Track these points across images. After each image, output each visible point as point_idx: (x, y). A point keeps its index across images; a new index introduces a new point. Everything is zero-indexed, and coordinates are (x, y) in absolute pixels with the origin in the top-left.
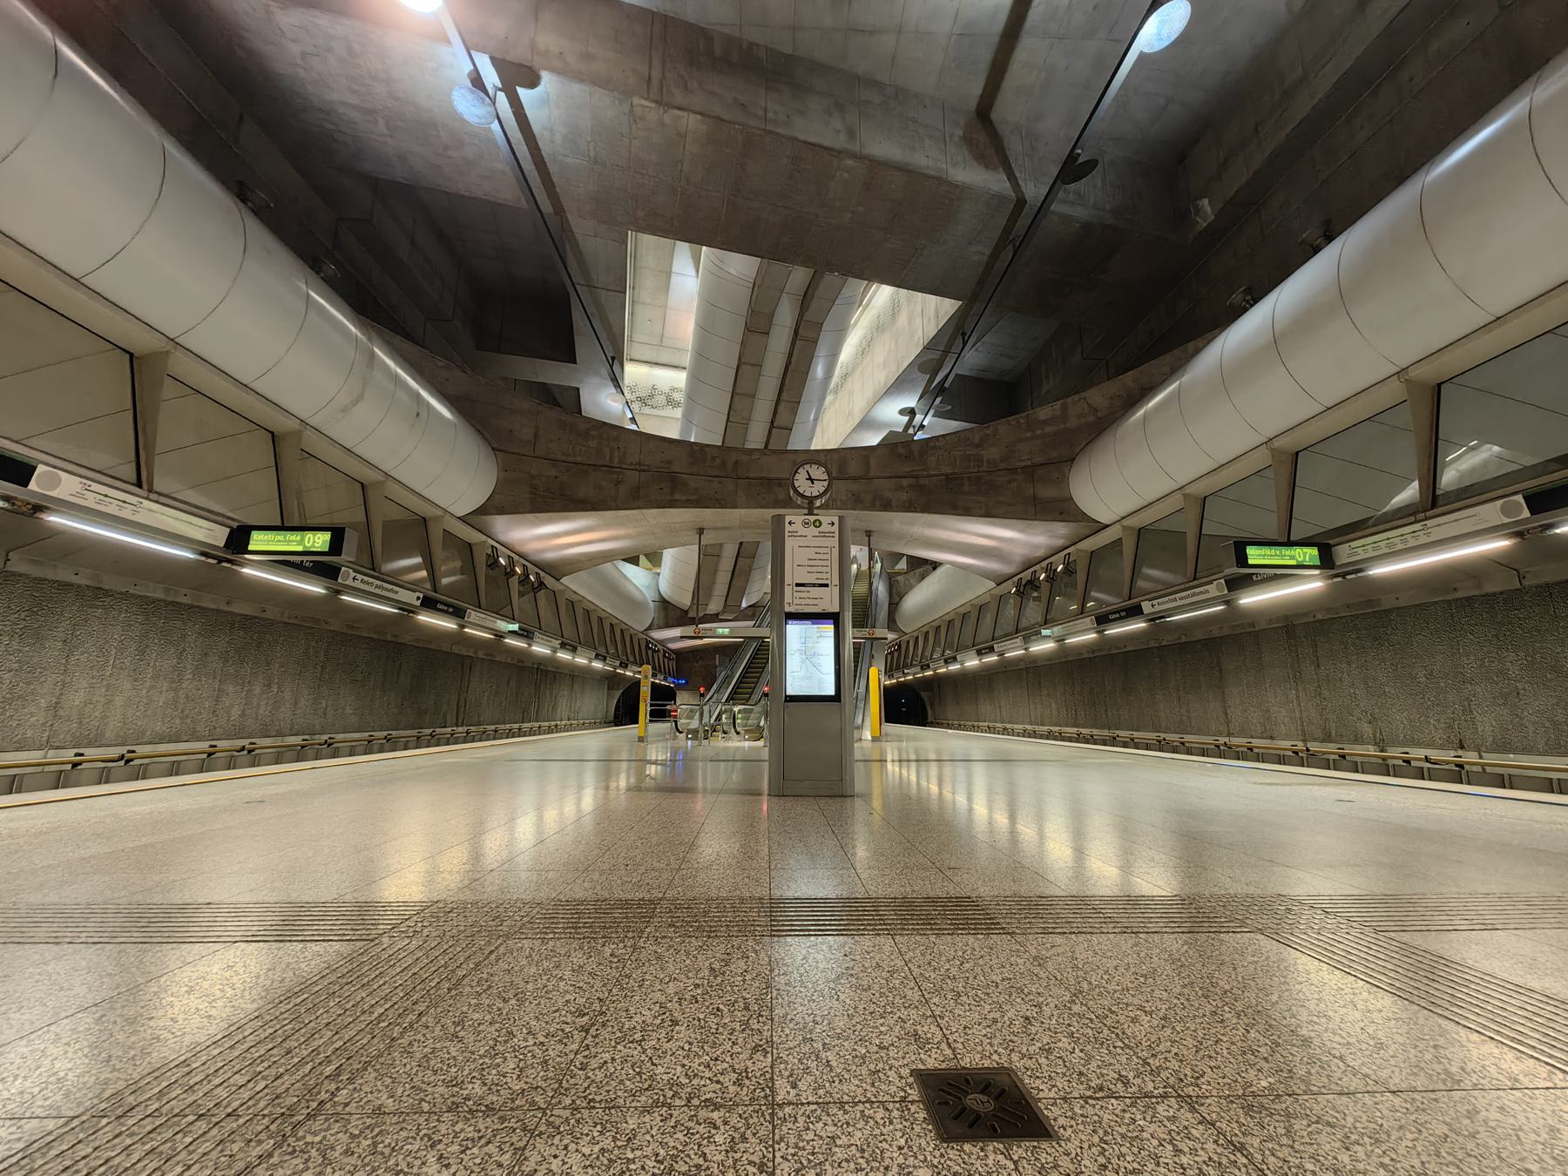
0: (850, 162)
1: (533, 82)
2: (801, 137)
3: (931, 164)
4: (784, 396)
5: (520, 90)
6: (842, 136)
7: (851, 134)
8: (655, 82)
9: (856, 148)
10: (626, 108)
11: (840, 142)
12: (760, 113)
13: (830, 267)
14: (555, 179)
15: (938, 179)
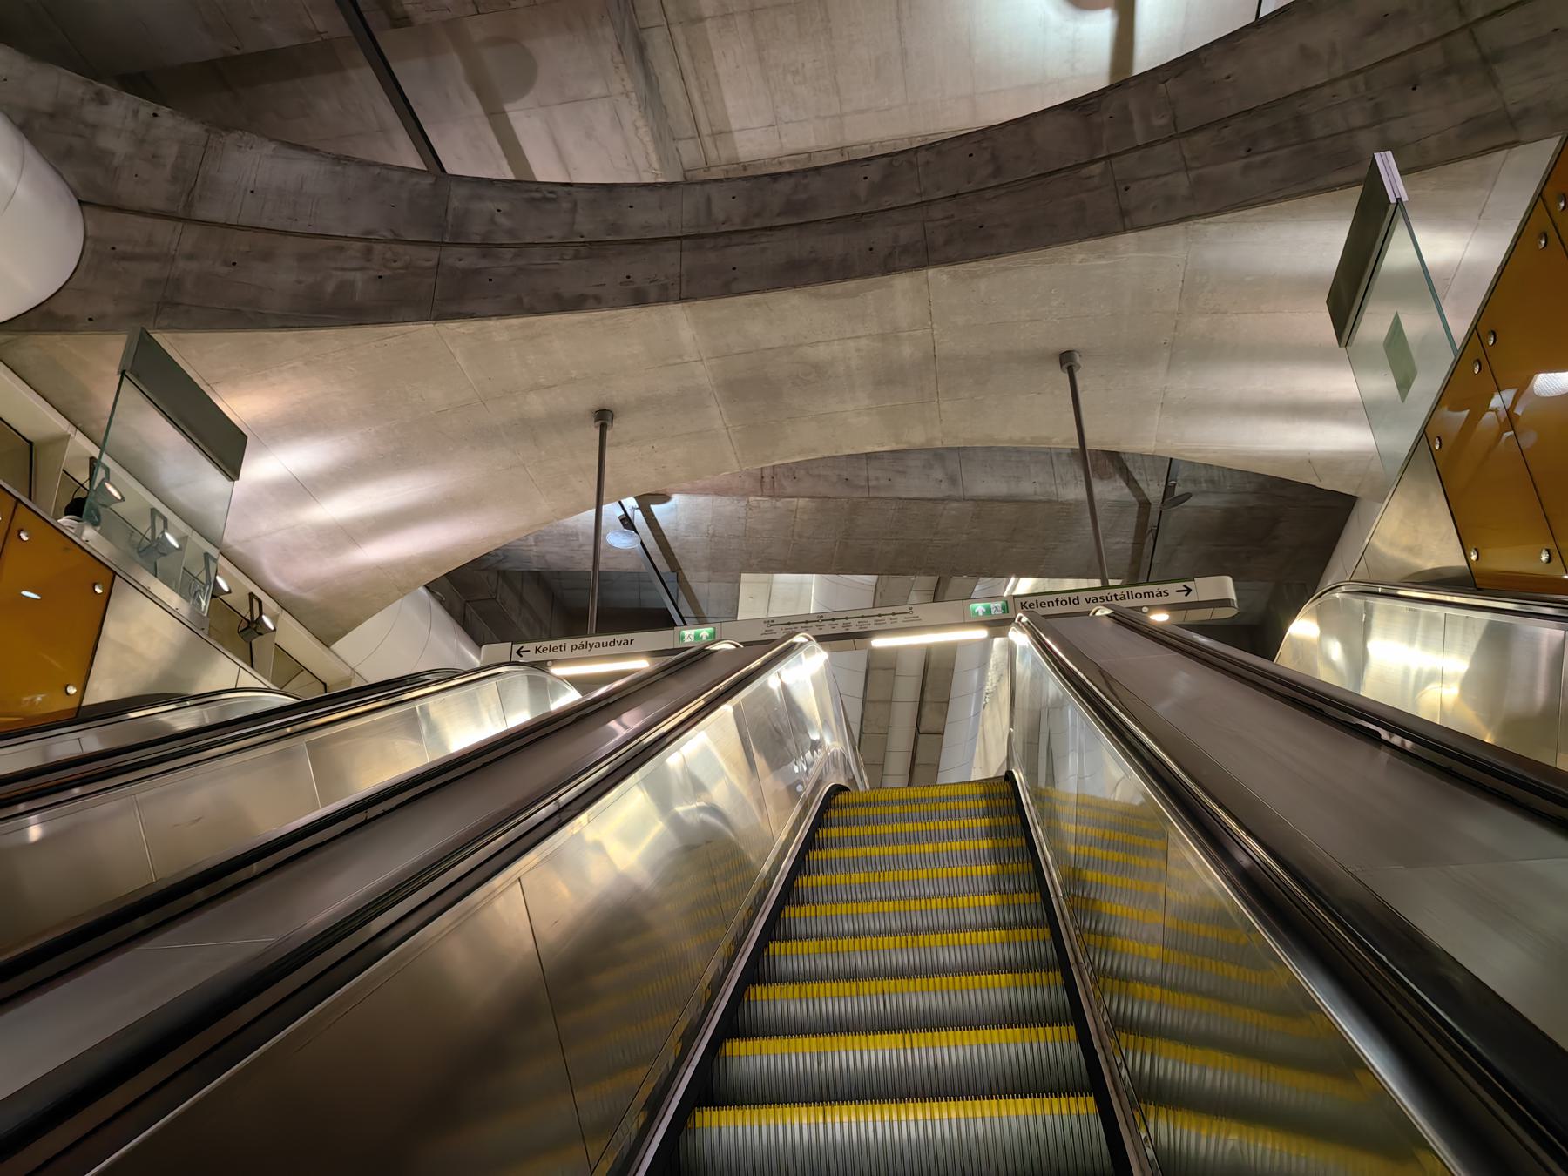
0: (955, 505)
1: (664, 498)
2: (904, 495)
3: (1039, 490)
4: (928, 697)
5: (654, 508)
6: (944, 486)
7: (953, 480)
8: (767, 480)
9: (958, 492)
10: (744, 503)
11: (944, 490)
12: (864, 483)
13: (956, 572)
14: (675, 551)
15: (1049, 502)
